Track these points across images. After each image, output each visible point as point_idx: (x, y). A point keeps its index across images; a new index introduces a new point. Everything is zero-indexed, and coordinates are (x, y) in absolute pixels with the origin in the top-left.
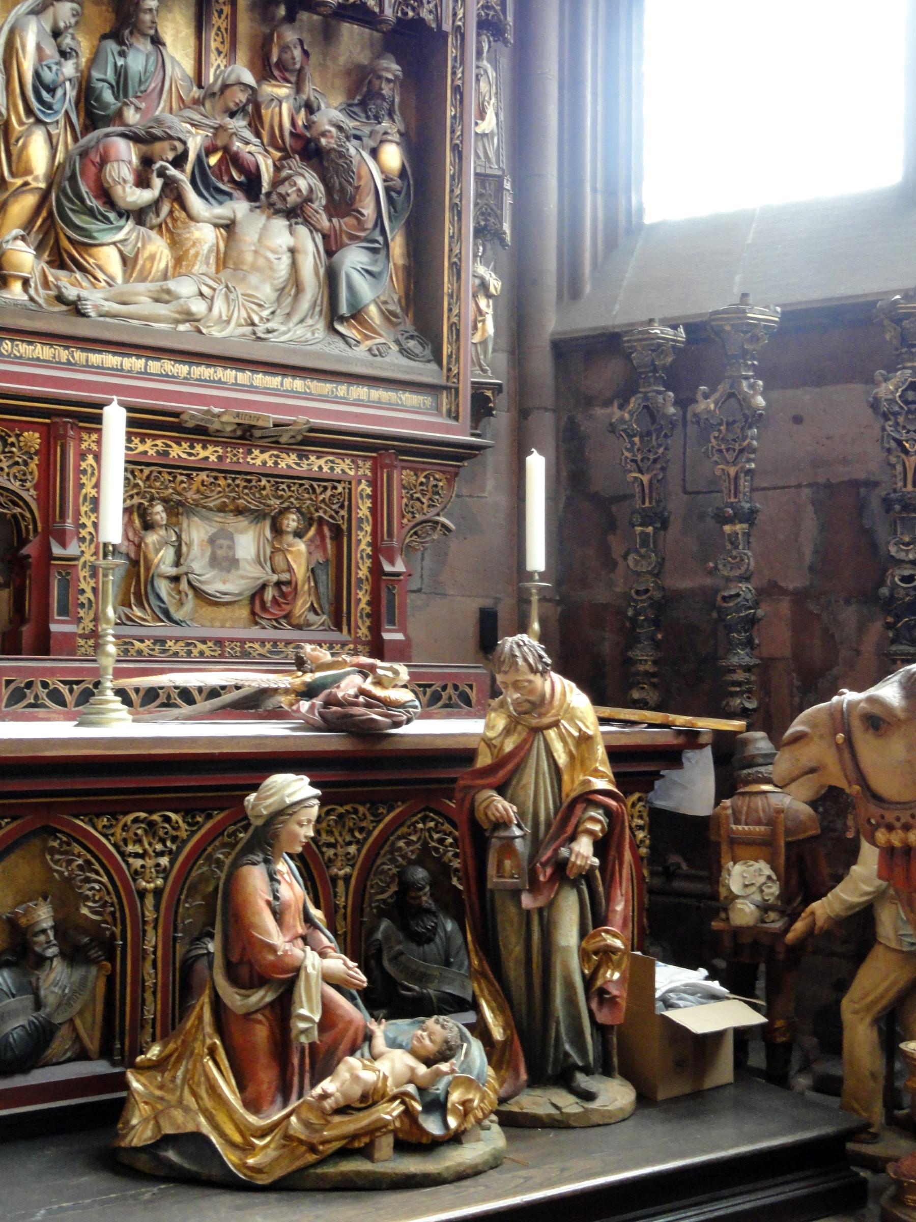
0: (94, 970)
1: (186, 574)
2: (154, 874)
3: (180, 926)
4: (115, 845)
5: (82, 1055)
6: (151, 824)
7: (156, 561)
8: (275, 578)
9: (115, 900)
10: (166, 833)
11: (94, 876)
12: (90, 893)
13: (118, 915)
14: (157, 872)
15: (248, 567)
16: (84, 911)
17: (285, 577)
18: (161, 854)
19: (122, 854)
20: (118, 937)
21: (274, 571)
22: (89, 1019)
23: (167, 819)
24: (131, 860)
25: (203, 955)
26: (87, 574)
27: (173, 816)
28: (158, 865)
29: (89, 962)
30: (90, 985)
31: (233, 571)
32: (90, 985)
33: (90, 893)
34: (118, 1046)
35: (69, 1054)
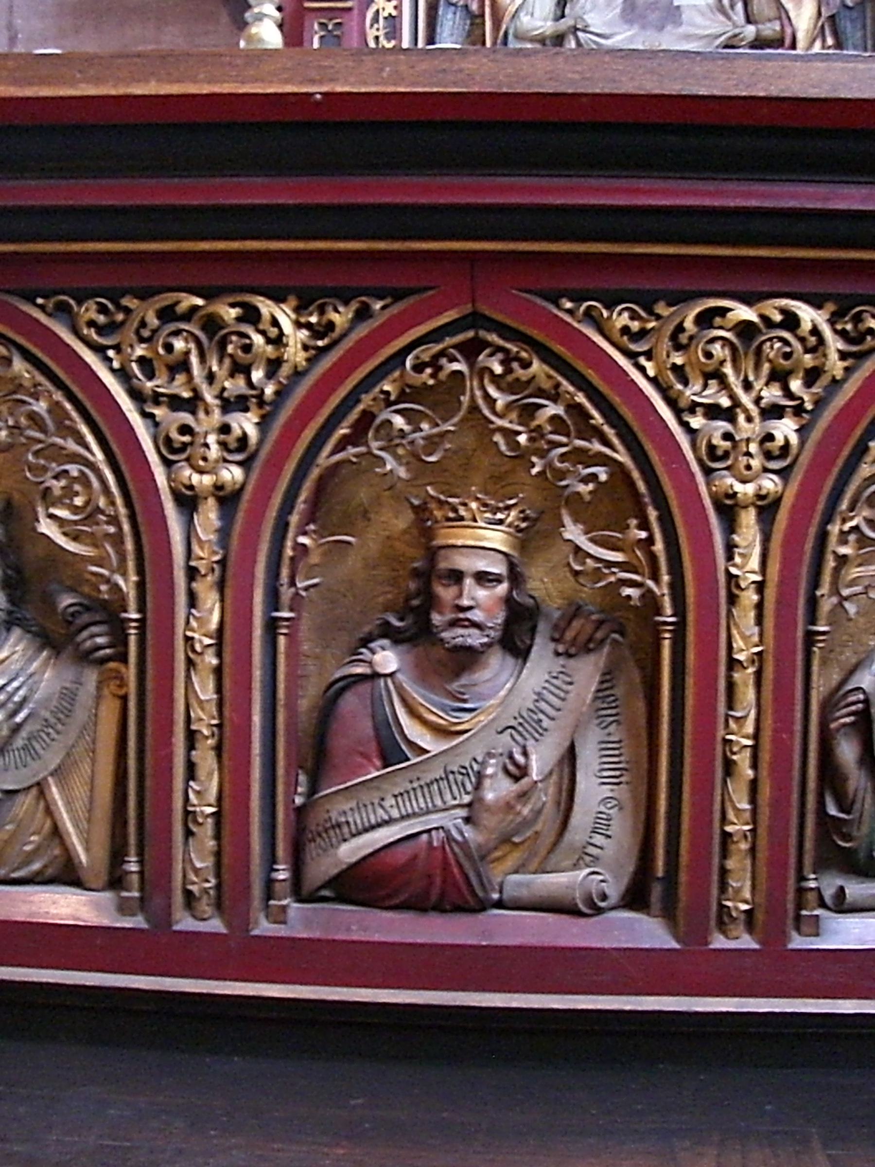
0: (91, 677)
1: (575, 29)
2: (214, 452)
3: (286, 593)
4: (123, 375)
5: (68, 875)
6: (212, 324)
7: (512, 9)
8: (750, 31)
9: (122, 511)
10: (247, 348)
11: (72, 445)
12: (58, 486)
13: (129, 546)
14: (223, 445)
15: (699, 20)
16: (46, 527)
17: (771, 29)
18: (240, 404)
19: (136, 395)
20: (132, 603)
21: (749, 21)
22: (80, 791)
23: (251, 315)
24: (159, 412)
25: (362, 678)
26: (381, 33)
27: (266, 307)
28: (225, 429)
29: (86, 657)
30: (81, 715)
31: (669, 28)
32: (81, 715)
33: (58, 486)
34: (134, 868)
35: (36, 866)
